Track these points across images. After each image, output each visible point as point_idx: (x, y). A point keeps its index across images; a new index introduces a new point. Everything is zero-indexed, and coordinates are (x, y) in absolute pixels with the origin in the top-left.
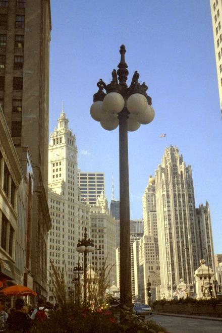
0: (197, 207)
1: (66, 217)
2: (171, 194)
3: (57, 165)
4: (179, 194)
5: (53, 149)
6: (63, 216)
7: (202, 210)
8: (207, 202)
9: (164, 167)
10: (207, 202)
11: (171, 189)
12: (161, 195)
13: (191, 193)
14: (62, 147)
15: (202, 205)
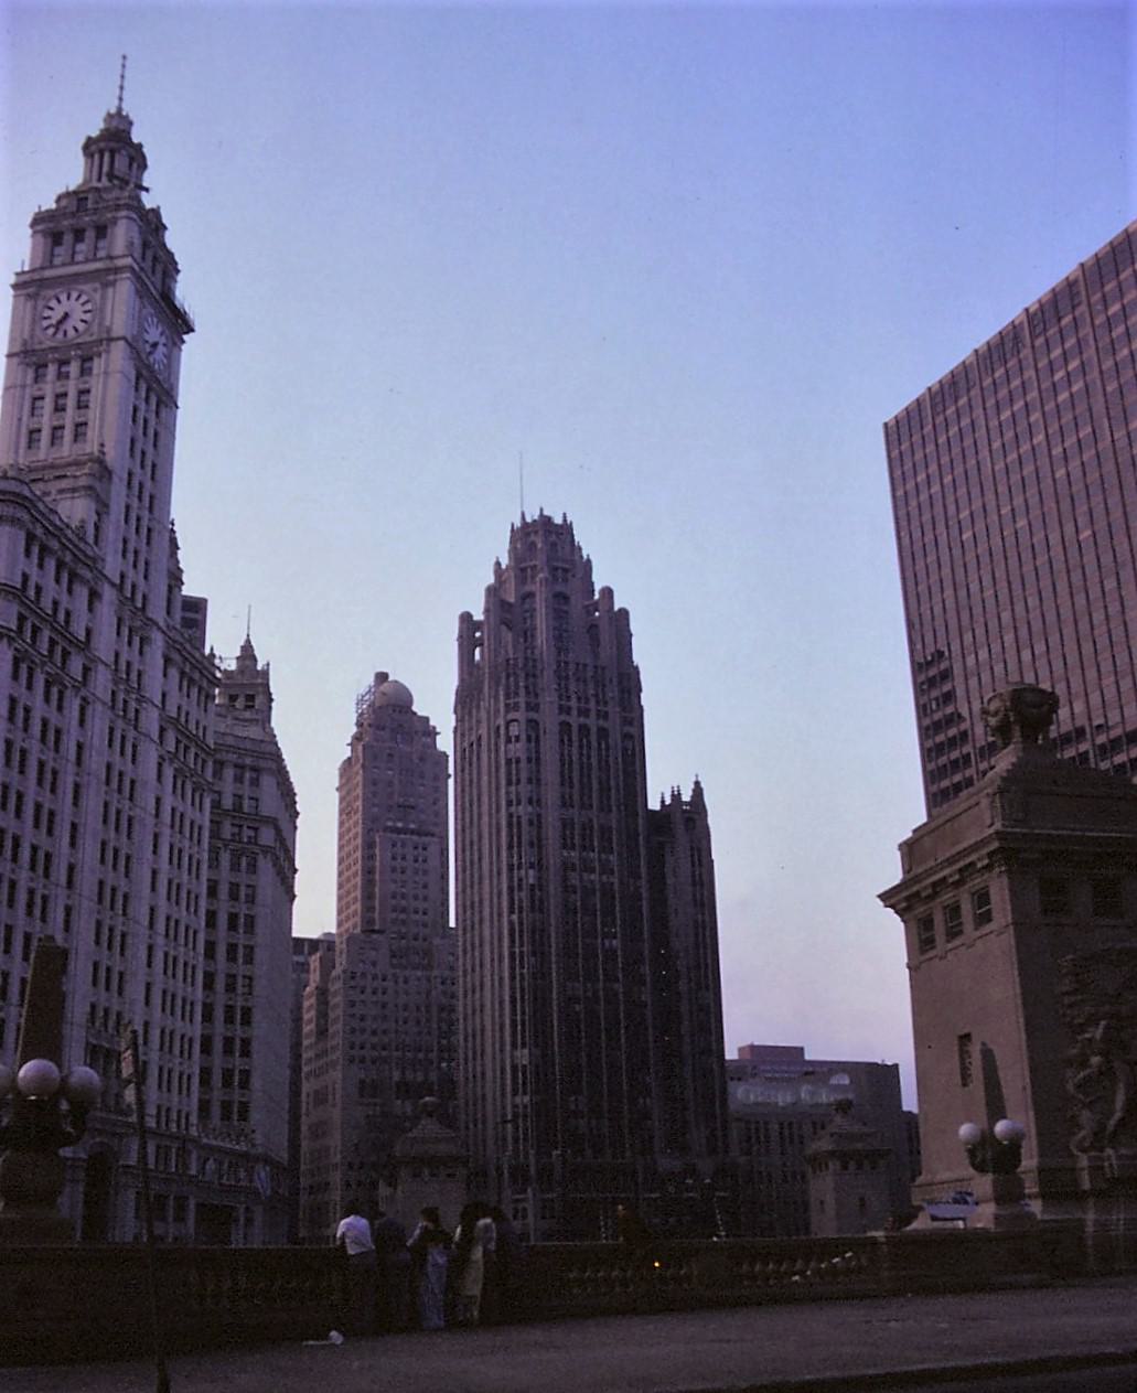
0: (654, 804)
1: (102, 682)
2: (549, 720)
3: (62, 376)
4: (584, 729)
5: (43, 283)
6: (86, 670)
7: (678, 818)
8: (697, 784)
9: (512, 600)
10: (697, 784)
11: (549, 700)
12: (501, 722)
13: (633, 730)
14: (108, 271)
15: (676, 797)
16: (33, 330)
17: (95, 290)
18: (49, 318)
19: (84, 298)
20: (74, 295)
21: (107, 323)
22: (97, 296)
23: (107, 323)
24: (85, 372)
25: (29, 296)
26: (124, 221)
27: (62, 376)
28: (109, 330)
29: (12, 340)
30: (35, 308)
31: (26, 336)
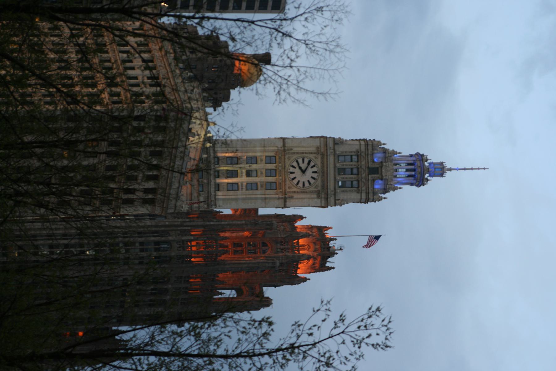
3: (269, 173)
16: (297, 153)
17: (316, 187)
18: (303, 162)
19: (312, 181)
20: (315, 175)
21: (295, 196)
22: (312, 189)
23: (295, 196)
24: (268, 186)
25: (318, 148)
26: (359, 197)
27: (269, 173)
28: (292, 197)
29: (293, 139)
30: (311, 153)
31: (295, 150)
